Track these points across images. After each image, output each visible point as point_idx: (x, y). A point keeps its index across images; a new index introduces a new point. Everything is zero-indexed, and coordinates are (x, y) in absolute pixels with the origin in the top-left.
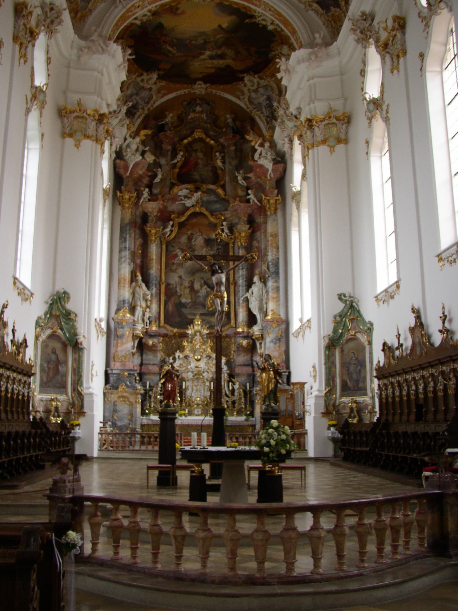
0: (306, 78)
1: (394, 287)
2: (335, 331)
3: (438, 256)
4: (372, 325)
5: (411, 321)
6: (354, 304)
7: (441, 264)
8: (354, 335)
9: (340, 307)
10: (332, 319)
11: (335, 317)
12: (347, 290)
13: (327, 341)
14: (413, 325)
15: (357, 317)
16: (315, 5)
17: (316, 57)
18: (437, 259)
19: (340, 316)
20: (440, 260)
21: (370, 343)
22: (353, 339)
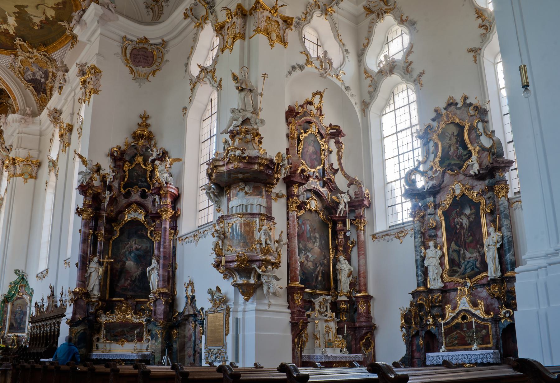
0: (17, 132)
1: (45, 272)
2: (10, 292)
3: (65, 261)
4: (33, 291)
5: (49, 293)
6: (24, 277)
7: (65, 265)
8: (22, 296)
9: (15, 278)
10: (9, 285)
11: (11, 284)
12: (21, 268)
13: (3, 298)
14: (49, 295)
15: (25, 285)
16: (31, 88)
17: (25, 121)
18: (64, 262)
19: (14, 283)
20: (66, 263)
21: (31, 301)
22: (21, 298)
